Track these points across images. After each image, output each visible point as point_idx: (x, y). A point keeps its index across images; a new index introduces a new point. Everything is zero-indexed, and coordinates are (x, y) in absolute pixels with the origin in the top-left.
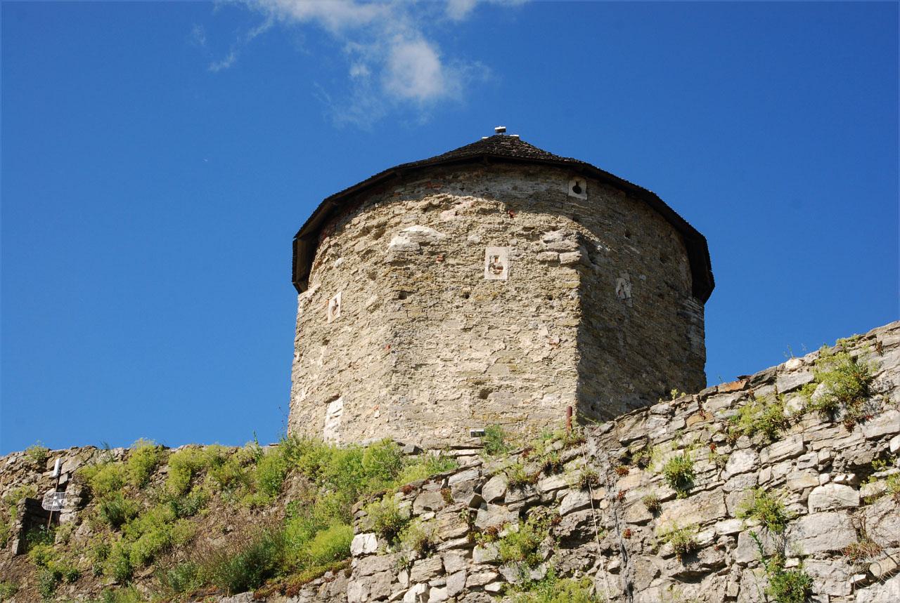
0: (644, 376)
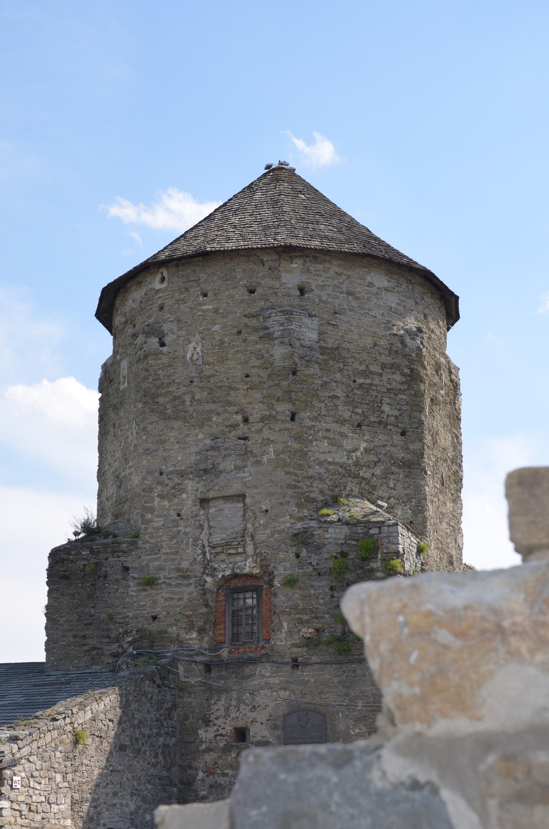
0: (214, 419)
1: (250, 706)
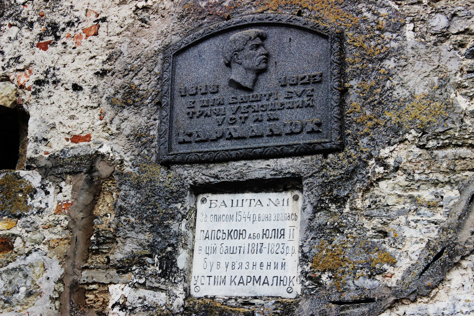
1: (38, 29)
